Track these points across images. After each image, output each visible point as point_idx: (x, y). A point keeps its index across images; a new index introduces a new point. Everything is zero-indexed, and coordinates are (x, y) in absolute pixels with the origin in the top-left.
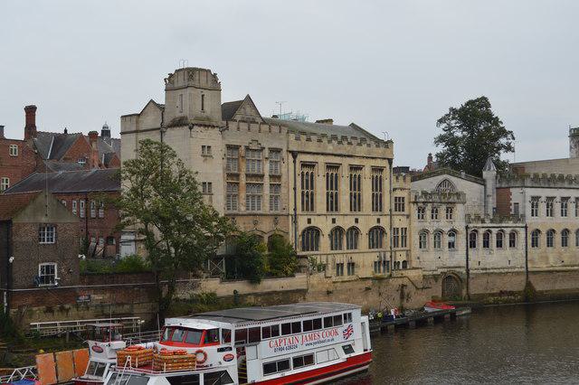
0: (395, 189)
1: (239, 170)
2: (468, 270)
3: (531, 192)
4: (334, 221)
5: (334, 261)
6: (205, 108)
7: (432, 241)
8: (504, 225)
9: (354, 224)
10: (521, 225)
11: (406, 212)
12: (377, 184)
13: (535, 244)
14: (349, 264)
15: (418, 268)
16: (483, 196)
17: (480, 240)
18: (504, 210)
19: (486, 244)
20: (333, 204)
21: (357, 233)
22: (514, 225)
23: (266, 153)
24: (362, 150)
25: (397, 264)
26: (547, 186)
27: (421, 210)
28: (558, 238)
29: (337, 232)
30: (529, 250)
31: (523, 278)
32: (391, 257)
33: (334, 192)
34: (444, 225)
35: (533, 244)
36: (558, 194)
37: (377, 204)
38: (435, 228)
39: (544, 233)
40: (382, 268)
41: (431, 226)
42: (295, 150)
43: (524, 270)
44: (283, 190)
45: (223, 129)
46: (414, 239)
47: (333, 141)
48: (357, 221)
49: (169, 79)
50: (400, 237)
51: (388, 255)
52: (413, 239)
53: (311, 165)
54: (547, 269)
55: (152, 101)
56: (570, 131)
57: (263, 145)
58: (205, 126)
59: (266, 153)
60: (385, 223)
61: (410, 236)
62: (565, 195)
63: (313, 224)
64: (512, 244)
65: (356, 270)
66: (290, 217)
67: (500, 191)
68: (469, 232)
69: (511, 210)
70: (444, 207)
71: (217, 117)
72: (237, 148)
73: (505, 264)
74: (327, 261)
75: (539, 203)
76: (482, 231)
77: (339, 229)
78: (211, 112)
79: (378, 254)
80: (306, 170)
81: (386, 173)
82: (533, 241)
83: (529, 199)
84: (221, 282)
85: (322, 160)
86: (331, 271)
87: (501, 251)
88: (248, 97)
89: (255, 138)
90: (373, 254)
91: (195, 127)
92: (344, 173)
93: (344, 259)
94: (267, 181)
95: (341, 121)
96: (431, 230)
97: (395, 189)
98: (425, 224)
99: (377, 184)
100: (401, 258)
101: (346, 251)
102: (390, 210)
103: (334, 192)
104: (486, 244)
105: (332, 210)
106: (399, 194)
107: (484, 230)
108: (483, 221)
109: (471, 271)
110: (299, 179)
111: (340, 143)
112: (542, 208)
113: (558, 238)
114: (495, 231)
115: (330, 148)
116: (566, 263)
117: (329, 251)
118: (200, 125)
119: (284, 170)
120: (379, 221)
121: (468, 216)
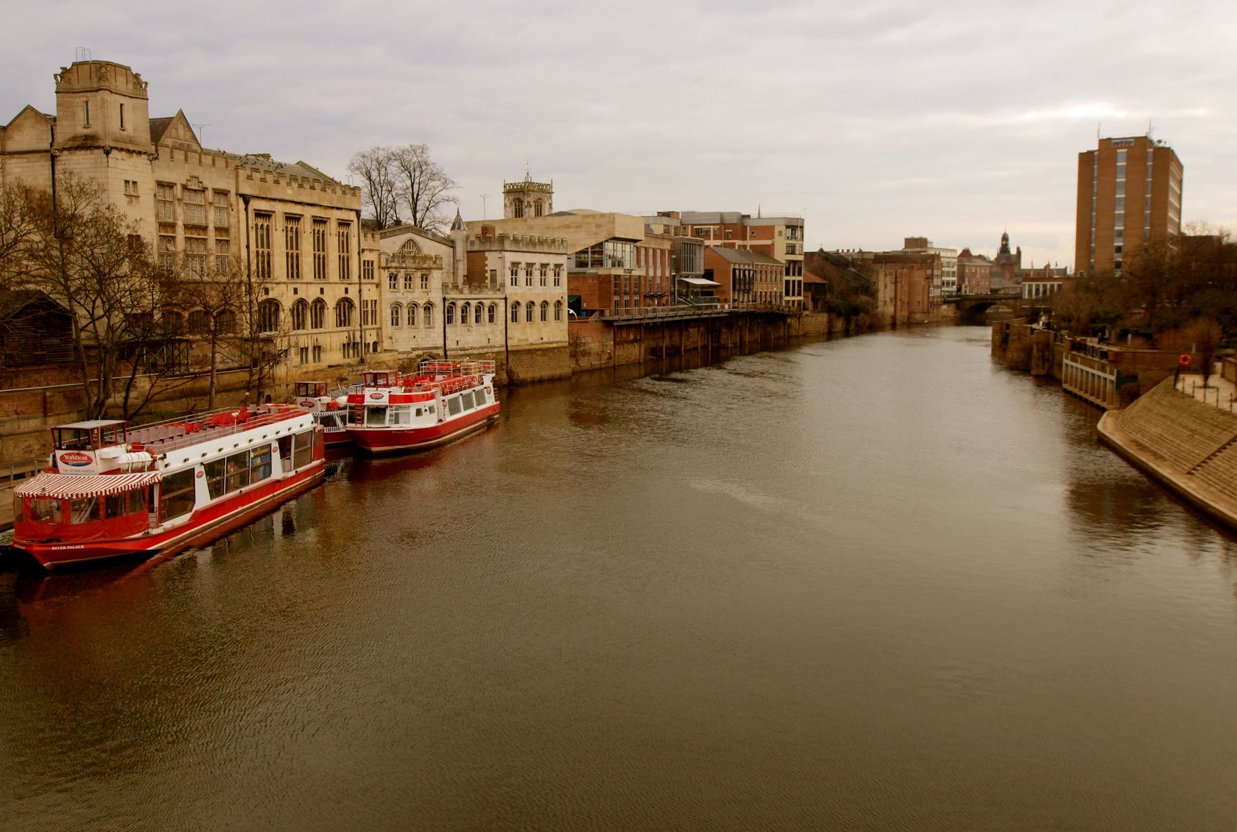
0: (363, 250)
1: (175, 218)
2: (445, 352)
3: (510, 257)
4: (296, 291)
6: (126, 125)
7: (406, 316)
9: (318, 295)
10: (499, 295)
11: (376, 280)
12: (344, 245)
13: (514, 319)
14: (314, 348)
15: (391, 351)
16: (452, 260)
17: (458, 314)
18: (476, 276)
19: (464, 320)
20: (294, 269)
21: (322, 308)
22: (494, 296)
23: (210, 193)
24: (327, 198)
25: (367, 345)
27: (393, 277)
28: (537, 311)
32: (361, 337)
33: (295, 252)
34: (419, 296)
35: (512, 318)
36: (538, 259)
37: (345, 272)
38: (409, 301)
39: (524, 305)
40: (351, 351)
41: (404, 297)
43: (504, 349)
44: (233, 249)
45: (153, 158)
46: (386, 314)
47: (293, 183)
48: (322, 291)
49: (62, 75)
50: (370, 313)
51: (358, 334)
52: (384, 314)
53: (266, 215)
54: (527, 347)
55: (29, 108)
56: (505, 187)
57: (206, 184)
58: (128, 151)
59: (210, 193)
60: (353, 294)
61: (381, 311)
62: (544, 262)
63: (271, 295)
64: (491, 319)
65: (322, 355)
67: (471, 254)
68: (447, 305)
69: (487, 278)
70: (419, 274)
71: (144, 137)
72: (171, 186)
73: (485, 343)
75: (519, 270)
76: (460, 304)
77: (302, 302)
78: (134, 130)
79: (346, 334)
80: (260, 222)
81: (354, 228)
82: (512, 315)
83: (508, 265)
85: (280, 208)
86: (294, 358)
88: (181, 115)
89: (195, 174)
90: (341, 334)
91: (114, 153)
92: (307, 226)
94: (212, 236)
95: (286, 157)
96: (405, 303)
97: (363, 250)
98: (397, 294)
99: (344, 245)
100: (371, 338)
102: (360, 277)
103: (295, 252)
104: (464, 320)
105: (292, 276)
106: (367, 256)
108: (461, 292)
109: (448, 353)
110: (252, 234)
111: (301, 186)
112: (522, 276)
113: (537, 311)
114: (474, 303)
115: (290, 193)
116: (545, 340)
118: (122, 150)
119: (233, 221)
121: (445, 286)
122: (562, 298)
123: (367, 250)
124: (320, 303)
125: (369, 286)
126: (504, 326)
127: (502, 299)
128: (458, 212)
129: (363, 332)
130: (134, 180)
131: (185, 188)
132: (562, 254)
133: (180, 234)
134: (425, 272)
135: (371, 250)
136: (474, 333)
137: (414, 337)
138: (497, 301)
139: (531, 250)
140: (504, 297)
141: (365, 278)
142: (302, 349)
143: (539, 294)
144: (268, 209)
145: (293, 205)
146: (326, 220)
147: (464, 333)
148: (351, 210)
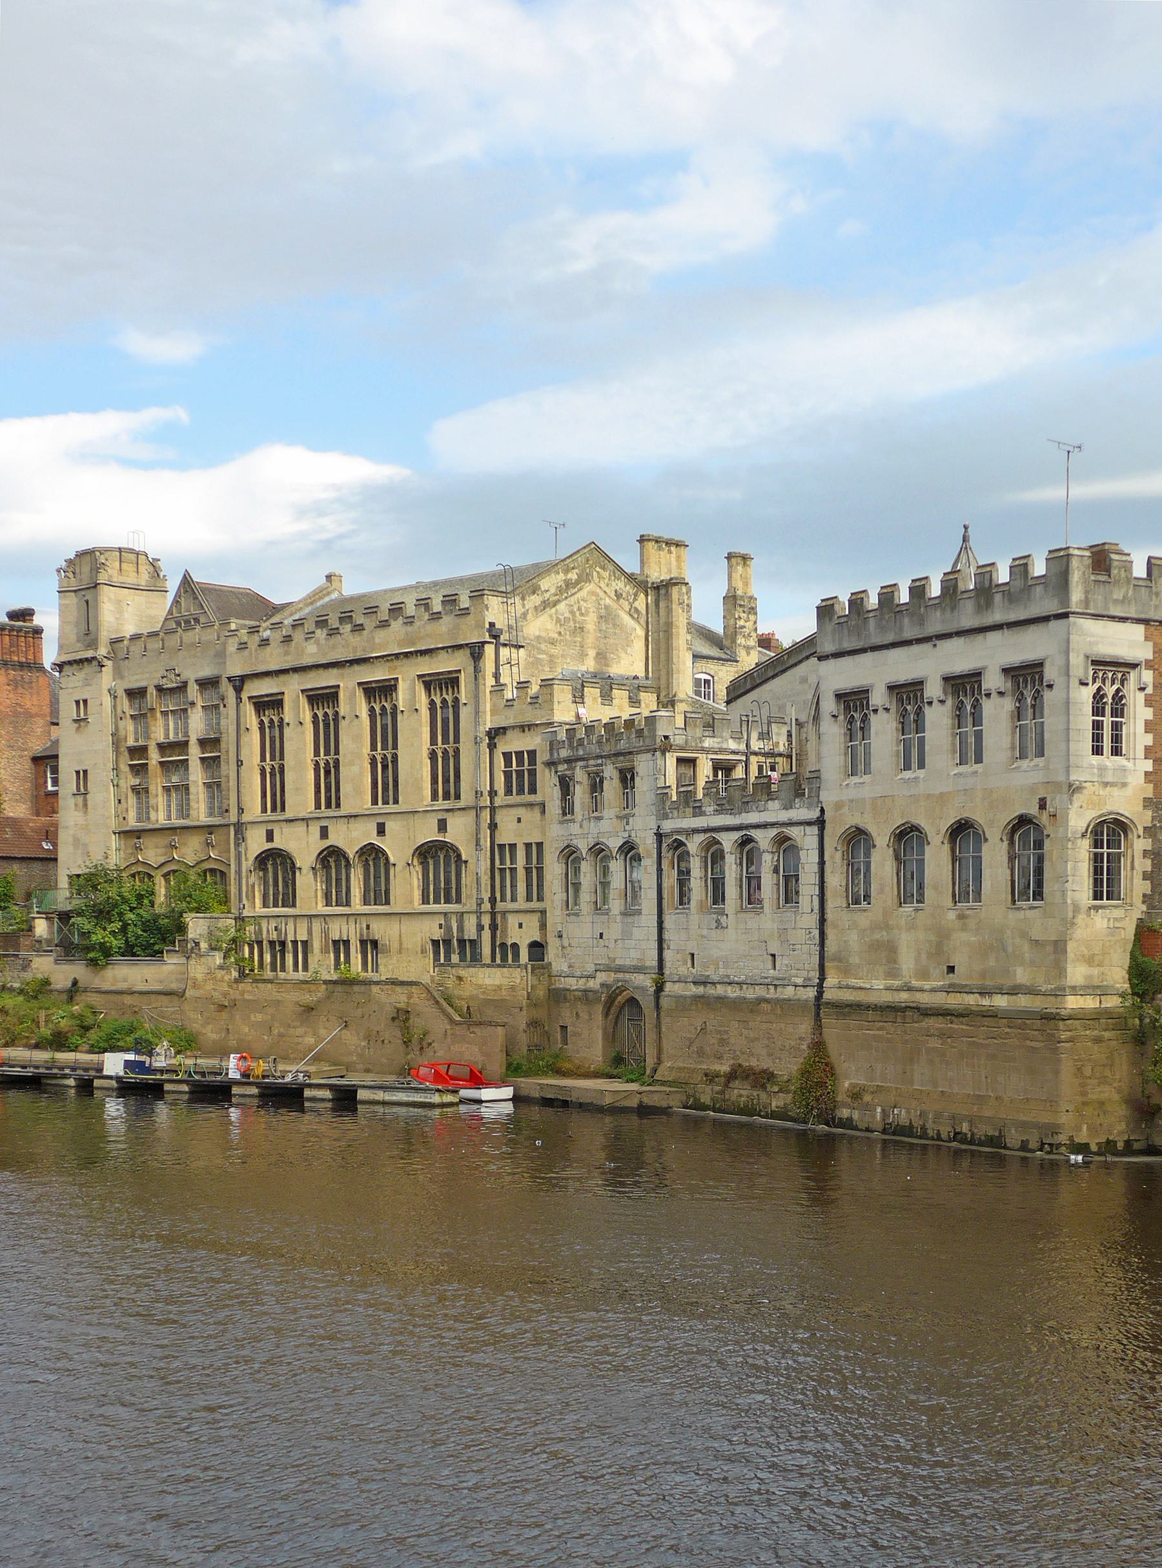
5: (326, 933)
8: (752, 818)
14: (363, 943)
22: (784, 816)
26: (890, 638)
27: (565, 785)
29: (331, 858)
30: (829, 916)
31: (804, 1027)
32: (480, 928)
42: (239, 673)
43: (811, 993)
48: (381, 830)
54: (887, 998)
62: (962, 666)
63: (277, 843)
66: (232, 829)
74: (310, 932)
84: (56, 962)
87: (752, 921)
89: (173, 664)
93: (351, 932)
94: (195, 752)
96: (583, 846)
101: (357, 905)
107: (699, 838)
109: (668, 987)
115: (311, 652)
117: (321, 909)
120: (442, 826)
122: (1043, 805)
123: (513, 727)
124: (372, 855)
125: (521, 812)
126: (816, 917)
127: (809, 823)
128: (965, 539)
129: (499, 917)
130: (84, 698)
131: (159, 689)
132: (1046, 619)
133: (154, 757)
134: (623, 763)
135: (524, 728)
136: (731, 931)
137: (601, 935)
138: (794, 832)
139: (908, 634)
140: (814, 814)
141: (508, 792)
142: (336, 943)
143: (943, 798)
144: (275, 690)
145: (321, 671)
146: (280, 697)
147: (705, 932)
148: (460, 647)
